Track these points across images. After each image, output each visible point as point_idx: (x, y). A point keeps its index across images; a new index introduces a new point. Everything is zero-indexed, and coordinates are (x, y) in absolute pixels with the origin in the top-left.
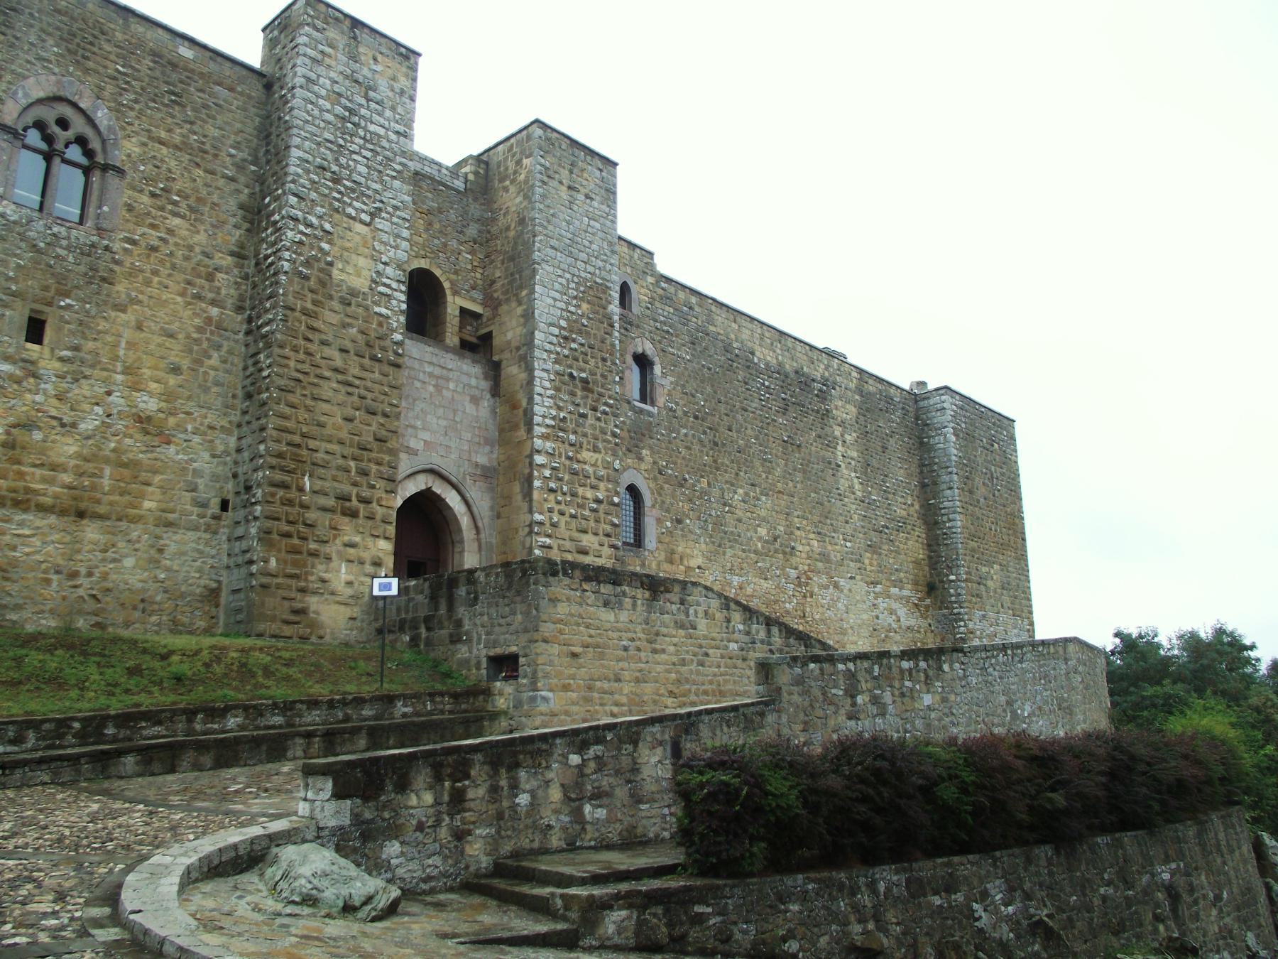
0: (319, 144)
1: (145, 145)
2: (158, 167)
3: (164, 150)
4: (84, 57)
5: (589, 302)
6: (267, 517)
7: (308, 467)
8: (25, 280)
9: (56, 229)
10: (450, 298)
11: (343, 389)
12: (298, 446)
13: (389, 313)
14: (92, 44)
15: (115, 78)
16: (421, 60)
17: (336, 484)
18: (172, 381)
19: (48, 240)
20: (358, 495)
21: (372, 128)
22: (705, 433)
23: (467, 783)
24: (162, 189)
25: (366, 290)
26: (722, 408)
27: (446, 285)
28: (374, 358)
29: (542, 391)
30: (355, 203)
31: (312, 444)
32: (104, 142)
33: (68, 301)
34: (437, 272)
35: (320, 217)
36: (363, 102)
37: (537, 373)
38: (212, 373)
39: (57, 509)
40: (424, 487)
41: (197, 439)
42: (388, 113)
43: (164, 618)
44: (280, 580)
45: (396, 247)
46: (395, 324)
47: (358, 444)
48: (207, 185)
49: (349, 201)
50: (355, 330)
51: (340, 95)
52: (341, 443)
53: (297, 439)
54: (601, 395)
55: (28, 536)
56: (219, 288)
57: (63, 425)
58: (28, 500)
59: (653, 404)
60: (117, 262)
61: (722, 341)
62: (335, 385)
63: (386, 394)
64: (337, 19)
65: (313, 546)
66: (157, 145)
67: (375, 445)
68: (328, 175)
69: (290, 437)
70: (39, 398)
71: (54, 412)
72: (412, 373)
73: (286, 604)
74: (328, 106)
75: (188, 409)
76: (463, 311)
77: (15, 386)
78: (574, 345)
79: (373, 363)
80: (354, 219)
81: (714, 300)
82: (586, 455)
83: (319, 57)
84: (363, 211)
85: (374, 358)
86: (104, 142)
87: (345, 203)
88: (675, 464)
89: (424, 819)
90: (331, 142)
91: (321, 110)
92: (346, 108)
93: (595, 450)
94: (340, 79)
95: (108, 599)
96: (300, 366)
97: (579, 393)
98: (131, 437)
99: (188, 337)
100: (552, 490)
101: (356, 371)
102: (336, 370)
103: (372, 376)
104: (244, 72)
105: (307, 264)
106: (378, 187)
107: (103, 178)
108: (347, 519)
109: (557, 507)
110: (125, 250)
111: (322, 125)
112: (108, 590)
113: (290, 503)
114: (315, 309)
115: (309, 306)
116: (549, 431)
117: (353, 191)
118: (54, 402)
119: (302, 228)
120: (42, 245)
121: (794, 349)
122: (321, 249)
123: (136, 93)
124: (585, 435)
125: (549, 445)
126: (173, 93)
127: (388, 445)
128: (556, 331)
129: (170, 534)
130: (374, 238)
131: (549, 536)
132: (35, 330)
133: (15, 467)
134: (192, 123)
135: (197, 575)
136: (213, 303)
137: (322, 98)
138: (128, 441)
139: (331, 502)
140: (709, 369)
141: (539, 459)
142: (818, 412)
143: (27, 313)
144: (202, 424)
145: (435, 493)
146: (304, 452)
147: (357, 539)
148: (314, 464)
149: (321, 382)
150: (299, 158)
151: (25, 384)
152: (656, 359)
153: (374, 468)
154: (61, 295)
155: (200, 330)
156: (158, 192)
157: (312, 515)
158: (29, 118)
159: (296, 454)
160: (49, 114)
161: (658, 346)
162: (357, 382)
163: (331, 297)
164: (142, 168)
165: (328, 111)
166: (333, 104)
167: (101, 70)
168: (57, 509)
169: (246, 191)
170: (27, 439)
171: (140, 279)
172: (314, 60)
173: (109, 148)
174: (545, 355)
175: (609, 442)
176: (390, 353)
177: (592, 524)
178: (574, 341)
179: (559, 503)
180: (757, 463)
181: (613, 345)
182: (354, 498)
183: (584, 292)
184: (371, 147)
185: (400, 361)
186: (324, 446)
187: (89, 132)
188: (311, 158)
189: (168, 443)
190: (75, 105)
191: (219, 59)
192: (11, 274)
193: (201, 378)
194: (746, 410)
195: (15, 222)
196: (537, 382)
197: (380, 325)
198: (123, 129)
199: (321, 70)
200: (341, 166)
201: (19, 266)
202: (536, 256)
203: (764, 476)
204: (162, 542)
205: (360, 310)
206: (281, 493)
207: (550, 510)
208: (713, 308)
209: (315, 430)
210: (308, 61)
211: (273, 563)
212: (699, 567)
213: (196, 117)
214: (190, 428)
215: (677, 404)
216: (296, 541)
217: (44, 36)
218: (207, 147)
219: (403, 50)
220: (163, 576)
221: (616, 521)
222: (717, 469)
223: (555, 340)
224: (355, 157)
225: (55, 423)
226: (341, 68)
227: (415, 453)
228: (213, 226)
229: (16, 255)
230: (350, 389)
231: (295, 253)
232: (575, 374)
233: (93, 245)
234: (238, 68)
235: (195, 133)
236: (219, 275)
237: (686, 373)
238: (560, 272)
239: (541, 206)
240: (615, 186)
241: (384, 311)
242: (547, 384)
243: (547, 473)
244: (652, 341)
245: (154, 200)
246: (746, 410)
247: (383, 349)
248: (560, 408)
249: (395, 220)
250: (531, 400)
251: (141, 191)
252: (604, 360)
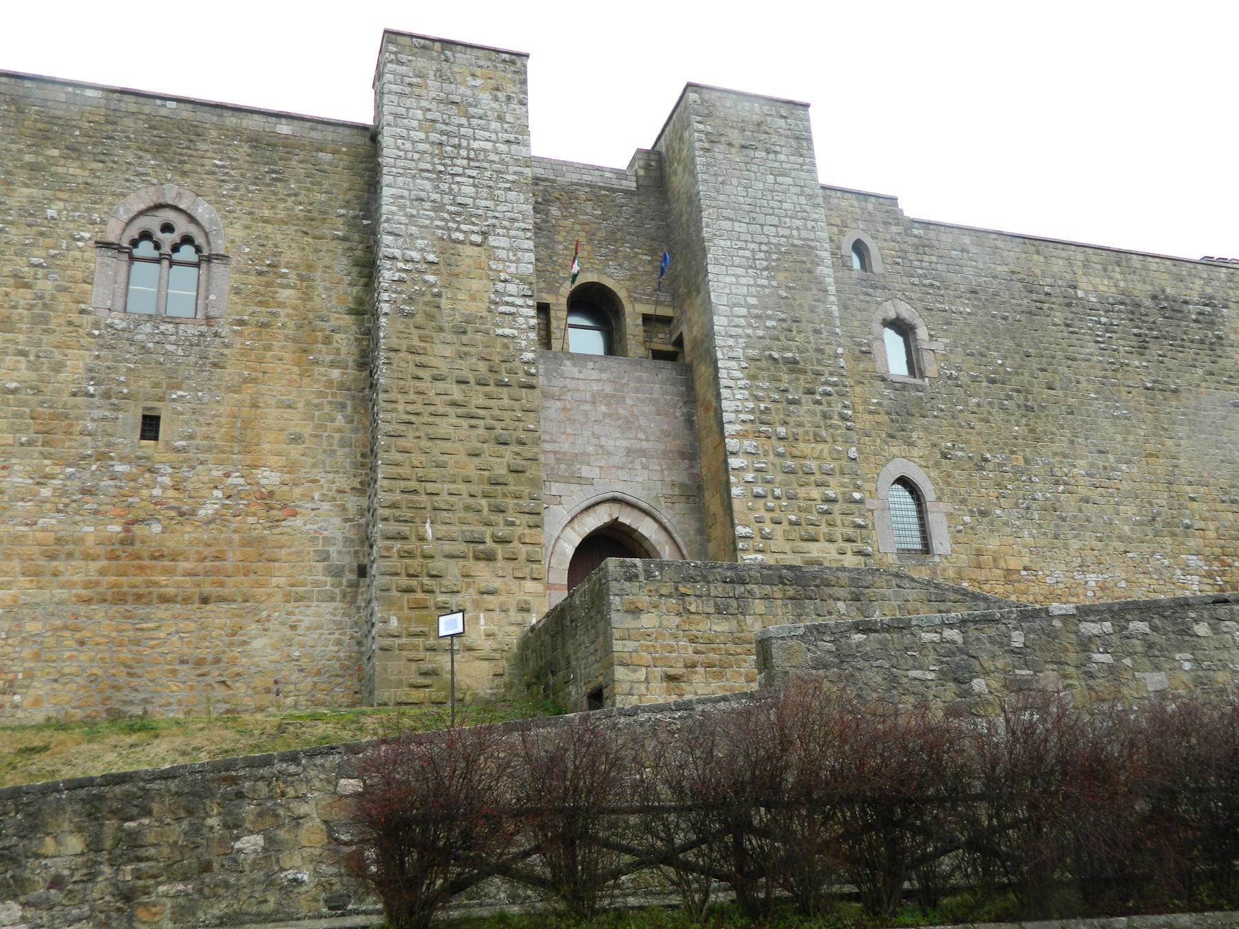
0: (414, 177)
1: (247, 227)
2: (263, 246)
4: (181, 162)
5: (786, 270)
6: (383, 574)
7: (428, 514)
8: (135, 381)
9: (162, 328)
10: (628, 308)
11: (465, 423)
12: (415, 492)
13: (515, 332)
14: (188, 148)
15: (213, 173)
16: (530, 64)
17: (465, 528)
18: (295, 451)
19: (157, 339)
20: (493, 536)
21: (475, 145)
22: (1009, 397)
23: (146, 821)
24: (269, 265)
25: (484, 314)
26: (1034, 364)
27: (622, 294)
28: (501, 384)
29: (732, 383)
30: (463, 227)
31: (431, 487)
32: (206, 234)
33: (180, 393)
34: (609, 283)
35: (422, 250)
36: (464, 121)
37: (720, 364)
38: (337, 436)
39: (179, 598)
40: (606, 519)
41: (326, 506)
42: (495, 125)
43: (301, 698)
44: (404, 640)
45: (518, 261)
46: (524, 343)
47: (489, 479)
48: (317, 251)
49: (455, 226)
51: (434, 121)
53: (413, 485)
54: (818, 374)
55: (152, 629)
56: (338, 349)
57: (182, 514)
58: (150, 593)
59: (922, 376)
60: (227, 346)
61: (1021, 281)
62: (455, 421)
64: (424, 47)
65: (441, 598)
66: (261, 224)
67: (511, 478)
68: (427, 205)
69: (403, 484)
70: (157, 492)
71: (173, 503)
72: (577, 396)
73: (413, 666)
74: (422, 135)
75: (314, 477)
76: (647, 318)
77: (132, 484)
78: (770, 323)
79: (500, 389)
80: (461, 242)
81: (1000, 234)
82: (803, 447)
83: (408, 90)
84: (473, 232)
85: (501, 384)
86: (206, 234)
87: (449, 229)
88: (967, 442)
89: (66, 872)
90: (428, 171)
91: (414, 142)
92: (442, 133)
93: (818, 439)
94: (434, 106)
95: (238, 684)
96: (410, 408)
97: (785, 377)
98: (254, 515)
99: (308, 404)
100: (758, 496)
101: (481, 401)
102: (454, 404)
103: (500, 403)
104: (348, 131)
105: (411, 300)
106: (490, 203)
107: (209, 270)
108: (482, 564)
109: (768, 516)
110: (235, 332)
111: (416, 156)
112: (238, 674)
113: (410, 554)
114: (423, 344)
115: (416, 343)
116: (748, 427)
117: (459, 214)
118: (171, 493)
119: (401, 265)
120: (151, 345)
121: (1145, 268)
122: (426, 282)
123: (236, 181)
124: (800, 425)
125: (749, 444)
126: (274, 172)
127: (527, 474)
128: (744, 311)
129: (302, 609)
130: (489, 257)
131: (761, 551)
132: (150, 426)
133: (136, 562)
134: (295, 195)
135: (336, 649)
136: (332, 365)
137: (414, 129)
138: (251, 519)
139: (461, 547)
140: (1005, 318)
141: (734, 462)
142: (1202, 342)
143: (139, 413)
144: (329, 490)
145: (623, 525)
146: (423, 498)
147: (497, 583)
148: (435, 509)
149: (437, 420)
150: (393, 196)
151: (141, 480)
152: (918, 322)
153: (511, 502)
154: (173, 388)
155: (321, 394)
156: (265, 269)
157: (437, 565)
158: (134, 232)
159: (412, 501)
160: (153, 223)
161: (919, 305)
162: (481, 412)
163: (441, 329)
164: (247, 250)
165: (421, 141)
166: (427, 133)
167: (199, 169)
168: (179, 598)
169: (360, 247)
170: (146, 533)
171: (253, 357)
172: (401, 94)
173: (211, 238)
174: (731, 342)
175: (837, 427)
176: (521, 374)
177: (824, 529)
178: (770, 318)
179: (771, 510)
180: (1106, 424)
181: (829, 313)
182: (488, 539)
183: (778, 259)
184: (477, 164)
185: (533, 381)
186: (446, 486)
187: (192, 230)
188: (406, 193)
189: (295, 515)
190: (175, 208)
191: (320, 126)
192: (122, 379)
193: (325, 443)
194: (1074, 359)
195: (123, 330)
196: (723, 374)
197: (505, 346)
198: (226, 217)
199: (410, 102)
200: (443, 193)
201: (129, 369)
202: (706, 233)
203: (1119, 438)
204: (294, 618)
205: (479, 336)
206: (398, 545)
207: (759, 521)
208: (1000, 244)
209: (434, 473)
210: (394, 98)
211: (394, 623)
212: (1025, 569)
213: (300, 188)
214: (317, 495)
215: (959, 369)
216: (420, 595)
217: (140, 153)
218: (315, 214)
219: (507, 57)
220: (297, 654)
221: (860, 521)
222: (1037, 440)
223: (742, 322)
224: (458, 179)
225: (173, 513)
226: (433, 94)
227: (590, 482)
228: (326, 289)
229: (126, 360)
230: (473, 422)
231: (395, 292)
232: (776, 355)
233: (202, 335)
234: (340, 130)
235: (300, 204)
236: (337, 336)
237: (968, 330)
238: (740, 244)
239: (705, 177)
240: (808, 130)
241: (507, 331)
242: (738, 374)
243: (749, 476)
244: (909, 300)
245: (261, 278)
246: (1074, 359)
247: (510, 372)
248: (758, 399)
249: (512, 233)
250: (718, 396)
251: (247, 273)
252: (817, 332)
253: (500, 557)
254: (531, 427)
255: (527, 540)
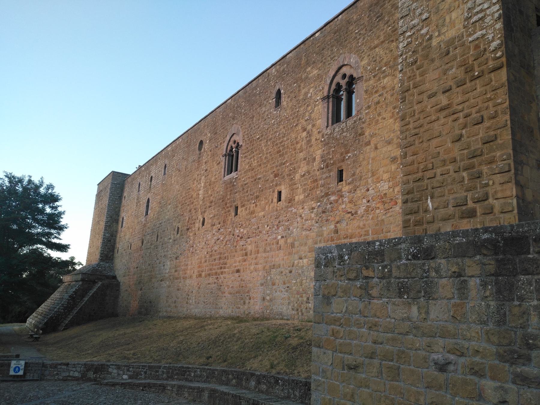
3: (377, 49)
20: (472, 199)
50: (454, 70)
52: (454, 161)
63: (490, 99)
153: (485, 169)
162: (460, 107)
253: (478, 214)
254: (499, 101)
255: (499, 195)
